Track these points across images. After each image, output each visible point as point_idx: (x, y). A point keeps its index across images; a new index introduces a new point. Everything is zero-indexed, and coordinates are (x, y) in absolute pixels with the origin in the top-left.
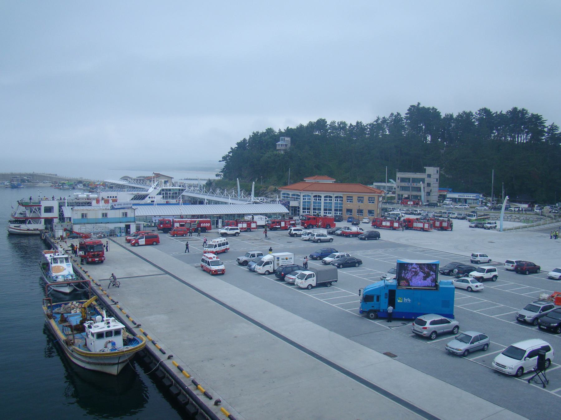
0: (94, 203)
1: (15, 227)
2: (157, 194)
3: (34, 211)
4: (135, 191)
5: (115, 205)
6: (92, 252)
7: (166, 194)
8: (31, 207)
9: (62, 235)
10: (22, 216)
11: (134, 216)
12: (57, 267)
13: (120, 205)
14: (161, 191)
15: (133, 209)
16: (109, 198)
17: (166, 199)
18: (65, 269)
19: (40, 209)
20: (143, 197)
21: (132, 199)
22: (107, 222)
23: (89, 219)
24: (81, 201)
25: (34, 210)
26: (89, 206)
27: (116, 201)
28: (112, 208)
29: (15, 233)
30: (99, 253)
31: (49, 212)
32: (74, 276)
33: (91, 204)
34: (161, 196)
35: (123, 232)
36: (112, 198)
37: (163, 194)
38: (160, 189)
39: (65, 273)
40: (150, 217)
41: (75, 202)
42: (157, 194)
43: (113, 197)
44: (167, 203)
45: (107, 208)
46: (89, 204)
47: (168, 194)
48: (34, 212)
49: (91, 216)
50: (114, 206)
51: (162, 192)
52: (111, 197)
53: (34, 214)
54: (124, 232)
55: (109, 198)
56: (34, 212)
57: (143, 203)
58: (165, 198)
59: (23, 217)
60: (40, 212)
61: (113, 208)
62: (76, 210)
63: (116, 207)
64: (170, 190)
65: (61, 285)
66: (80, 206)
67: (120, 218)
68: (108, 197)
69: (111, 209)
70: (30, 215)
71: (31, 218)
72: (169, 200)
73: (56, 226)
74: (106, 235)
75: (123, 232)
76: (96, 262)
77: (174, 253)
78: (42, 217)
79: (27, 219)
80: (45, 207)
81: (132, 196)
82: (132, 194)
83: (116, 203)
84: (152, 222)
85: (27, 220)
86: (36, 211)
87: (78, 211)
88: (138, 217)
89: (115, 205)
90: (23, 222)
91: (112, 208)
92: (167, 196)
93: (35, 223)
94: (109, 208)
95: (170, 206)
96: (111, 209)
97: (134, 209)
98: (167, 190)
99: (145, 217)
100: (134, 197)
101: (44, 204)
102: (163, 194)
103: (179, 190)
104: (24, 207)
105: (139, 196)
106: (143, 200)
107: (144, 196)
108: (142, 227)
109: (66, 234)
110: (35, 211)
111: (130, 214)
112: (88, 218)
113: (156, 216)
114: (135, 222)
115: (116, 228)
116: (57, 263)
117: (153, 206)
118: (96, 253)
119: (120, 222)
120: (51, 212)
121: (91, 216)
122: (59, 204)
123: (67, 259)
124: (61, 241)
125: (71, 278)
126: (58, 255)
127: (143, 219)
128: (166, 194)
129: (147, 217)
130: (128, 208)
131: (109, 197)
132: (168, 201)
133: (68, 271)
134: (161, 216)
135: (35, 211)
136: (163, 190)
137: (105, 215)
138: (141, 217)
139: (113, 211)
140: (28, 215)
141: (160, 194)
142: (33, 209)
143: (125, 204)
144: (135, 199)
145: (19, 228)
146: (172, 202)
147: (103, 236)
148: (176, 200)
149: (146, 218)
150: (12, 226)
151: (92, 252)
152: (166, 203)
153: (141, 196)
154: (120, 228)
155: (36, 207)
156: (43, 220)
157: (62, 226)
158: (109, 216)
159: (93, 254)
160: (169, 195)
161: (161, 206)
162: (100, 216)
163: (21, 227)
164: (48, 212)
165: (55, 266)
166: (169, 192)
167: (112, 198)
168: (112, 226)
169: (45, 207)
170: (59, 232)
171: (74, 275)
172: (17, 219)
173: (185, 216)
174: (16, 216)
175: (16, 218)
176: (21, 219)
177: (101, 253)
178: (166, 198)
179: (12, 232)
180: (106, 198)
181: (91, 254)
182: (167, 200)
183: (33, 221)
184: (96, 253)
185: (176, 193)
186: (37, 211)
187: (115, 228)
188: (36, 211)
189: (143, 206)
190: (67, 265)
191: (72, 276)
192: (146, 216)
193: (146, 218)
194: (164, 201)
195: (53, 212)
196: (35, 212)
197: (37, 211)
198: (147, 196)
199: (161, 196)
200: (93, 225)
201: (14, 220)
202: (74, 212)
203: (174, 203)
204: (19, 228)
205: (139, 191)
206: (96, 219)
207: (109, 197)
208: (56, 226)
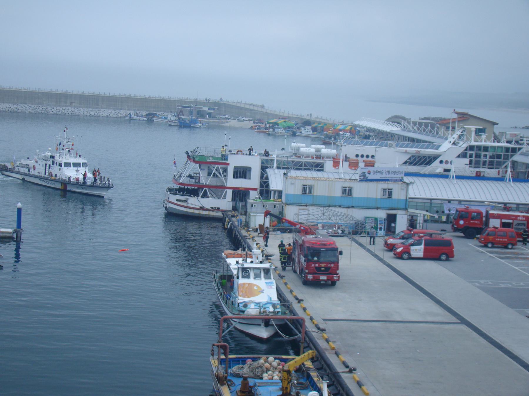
0: (329, 165)
1: (177, 200)
2: (459, 156)
3: (214, 173)
4: (411, 147)
5: (369, 173)
6: (315, 262)
7: (478, 156)
8: (209, 165)
9: (262, 223)
10: (192, 181)
11: (405, 198)
12: (247, 285)
13: (378, 174)
14: (466, 150)
15: (405, 183)
16: (359, 158)
17: (475, 167)
18: (262, 291)
19: (225, 170)
20: (428, 160)
21: (405, 163)
22: (351, 205)
23: (316, 196)
24: (304, 160)
25: (214, 171)
26: (318, 170)
27: (372, 164)
28: (362, 178)
29: (179, 213)
30: (329, 265)
31: (242, 178)
32: (279, 306)
33: (322, 167)
34: (467, 161)
35: (381, 229)
36: (365, 158)
37: (471, 156)
38: (465, 146)
39: (262, 298)
40: (439, 202)
41: (293, 162)
42: (459, 156)
43: (367, 156)
44: (478, 177)
45: (353, 178)
46: (319, 167)
47: (482, 157)
48: (215, 175)
49: (320, 191)
50: (367, 175)
51: (469, 153)
52: (362, 156)
53: (215, 179)
54: (383, 228)
55: (359, 158)
56: (215, 175)
57: (427, 173)
58: (475, 164)
59: (194, 184)
60: (226, 177)
61: (364, 178)
62: (292, 178)
63: (370, 177)
64: (486, 149)
65: (252, 321)
66: (301, 169)
67: (376, 199)
68: (357, 156)
69: (360, 181)
70: (206, 181)
71: (210, 187)
72: (481, 170)
73: (252, 206)
74: (347, 232)
75: (381, 229)
76: (322, 282)
77: (482, 282)
78: (228, 185)
79: (201, 187)
80: (235, 168)
81: (406, 158)
82: (406, 152)
83: (370, 169)
84: (443, 212)
85: (201, 190)
86: (218, 174)
87: (295, 179)
88: (414, 200)
89: (369, 173)
90: (194, 193)
91: (362, 178)
92: (479, 161)
93: (215, 196)
94: (357, 177)
95: (484, 182)
96: (360, 181)
97: (408, 184)
98: (479, 148)
99: (429, 201)
100: (410, 159)
101: (235, 161)
102: (471, 156)
103: (507, 149)
104: (198, 165)
105: (419, 157)
106: (428, 167)
107: (429, 157)
108: (420, 221)
109: (270, 223)
110: (216, 173)
111: (398, 194)
112: (315, 194)
113: (452, 202)
114: (406, 209)
115: (367, 219)
116: (248, 277)
117: (446, 180)
118: (323, 265)
119: (377, 208)
120: (245, 178)
121: (320, 191)
122: (262, 163)
123: (267, 271)
124: (260, 235)
125: (271, 309)
126: (252, 262)
127: (425, 206)
128: (478, 156)
129: (433, 201)
130: (395, 181)
131: (360, 155)
132: (480, 172)
133: (268, 296)
134: (462, 203)
135: (216, 173)
136: (471, 148)
137: (347, 191)
138: (421, 201)
139: (365, 184)
140: (204, 180)
141: (463, 155)
142: (212, 169)
143: (389, 172)
144: (410, 163)
146: (488, 174)
147: (340, 232)
148: (497, 170)
149: (431, 203)
150: (174, 198)
151: (315, 262)
152: (474, 175)
153: (424, 157)
154: (376, 219)
155: (219, 166)
156: (229, 193)
157: (264, 206)
158: (356, 194)
159: (317, 265)
160: (483, 159)
161: (463, 181)
162: (338, 193)
163: (189, 201)
164: (240, 178)
165: (244, 284)
166: (483, 153)
167: (365, 158)
168: (359, 215)
169: (235, 168)
170: (257, 217)
171: (278, 304)
172: (183, 187)
173: (515, 206)
174: (181, 181)
175: (181, 184)
176: (189, 187)
177: (332, 265)
178: (477, 164)
179: (173, 211)
180: (352, 157)
181: (313, 265)
182: (478, 170)
183: (211, 192)
184: (323, 265)
185: (499, 156)
186: (220, 174)
187: (366, 218)
188: (218, 174)
189: (426, 179)
190: (267, 283)
191: (274, 306)
192: (431, 199)
193: (431, 203)
194: (472, 171)
195: (250, 178)
196: (217, 176)
197: (220, 174)
198: (435, 158)
199: (467, 161)
200: (322, 209)
201: (177, 187)
202: (289, 181)
203: (492, 175)
205: (421, 148)
206: (329, 198)
207: (360, 155)
208: (252, 206)
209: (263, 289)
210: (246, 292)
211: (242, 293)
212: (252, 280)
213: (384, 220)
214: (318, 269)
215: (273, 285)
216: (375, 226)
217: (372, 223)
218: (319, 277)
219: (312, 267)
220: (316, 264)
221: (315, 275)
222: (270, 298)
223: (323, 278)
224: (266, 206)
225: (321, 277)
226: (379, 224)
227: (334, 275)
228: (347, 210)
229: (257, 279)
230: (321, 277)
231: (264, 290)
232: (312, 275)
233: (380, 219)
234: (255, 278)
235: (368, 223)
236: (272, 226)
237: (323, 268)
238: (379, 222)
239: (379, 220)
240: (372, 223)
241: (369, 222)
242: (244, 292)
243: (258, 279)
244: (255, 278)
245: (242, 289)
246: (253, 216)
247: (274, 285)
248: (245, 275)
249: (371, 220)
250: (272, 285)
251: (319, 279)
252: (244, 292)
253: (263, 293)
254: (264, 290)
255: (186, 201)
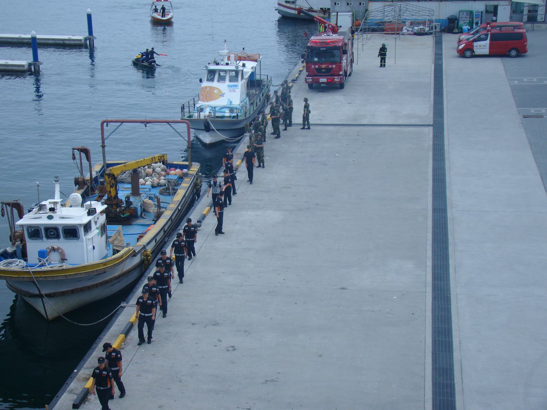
6: (315, 63)
18: (222, 95)
29: (288, 16)
30: (330, 66)
76: (322, 85)
118: (323, 66)
133: (229, 100)
145: (293, 6)
151: (315, 63)
157: (348, 4)
159: (317, 67)
165: (206, 87)
177: (334, 66)
181: (313, 67)
184: (323, 66)
190: (229, 86)
204: (293, 6)
209: (223, 92)
210: (206, 96)
211: (202, 97)
212: (215, 84)
213: (480, 13)
214: (319, 70)
215: (237, 88)
216: (469, 21)
217: (466, 18)
218: (319, 79)
219: (312, 69)
220: (316, 64)
221: (314, 77)
222: (231, 102)
223: (323, 80)
224: (351, 4)
225: (320, 79)
226: (474, 19)
227: (335, 77)
228: (439, 4)
229: (221, 82)
230: (320, 79)
231: (224, 94)
232: (311, 78)
233: (476, 12)
234: (218, 81)
235: (462, 18)
236: (354, 26)
237: (323, 69)
238: (474, 17)
239: (475, 13)
240: (466, 18)
241: (463, 16)
242: (204, 96)
243: (222, 82)
244: (218, 81)
245: (203, 93)
246: (333, 15)
247: (238, 89)
248: (210, 78)
249: (465, 14)
250: (236, 88)
251: (319, 82)
252: (204, 96)
253: (224, 96)
254: (224, 94)
255: (295, 3)
